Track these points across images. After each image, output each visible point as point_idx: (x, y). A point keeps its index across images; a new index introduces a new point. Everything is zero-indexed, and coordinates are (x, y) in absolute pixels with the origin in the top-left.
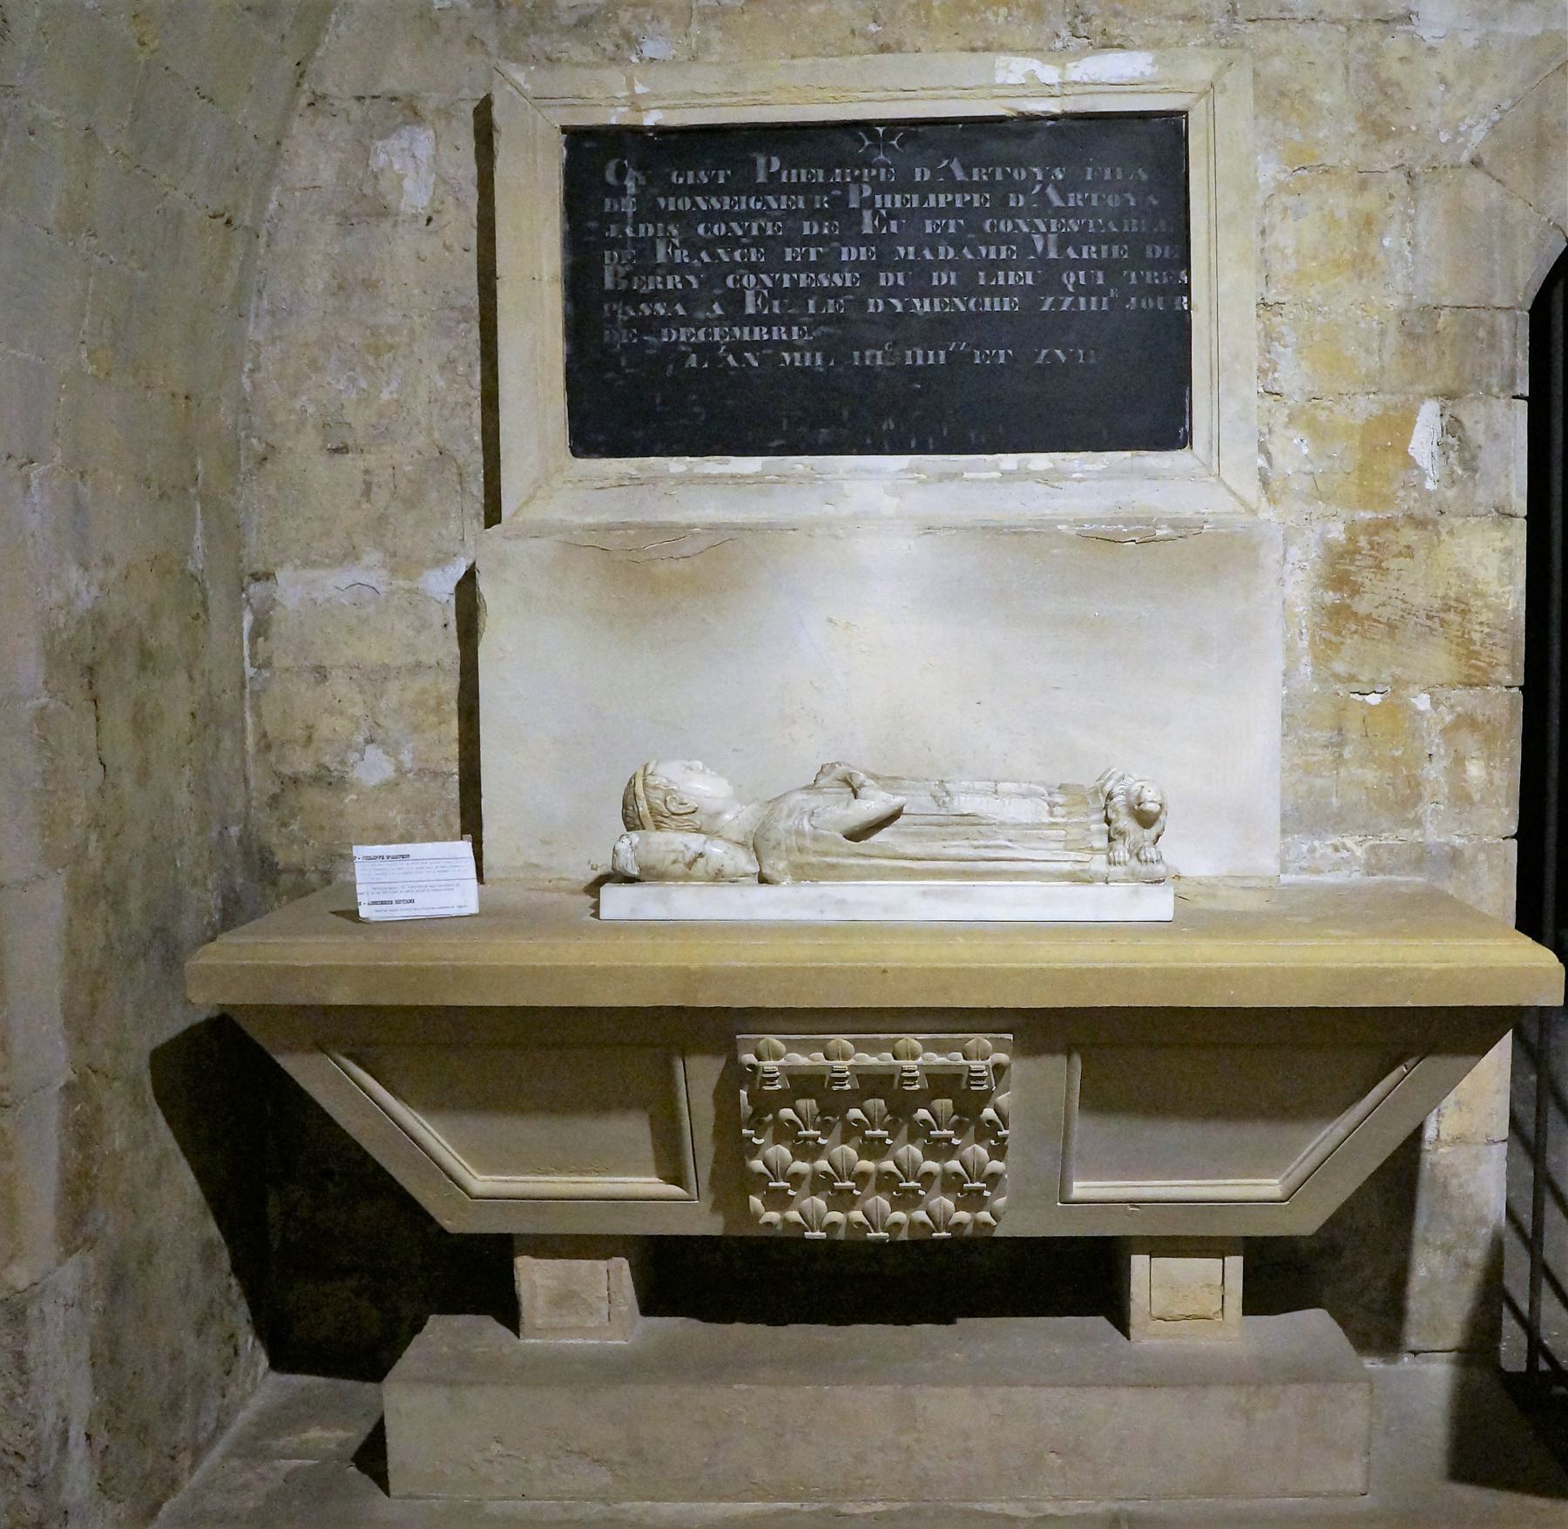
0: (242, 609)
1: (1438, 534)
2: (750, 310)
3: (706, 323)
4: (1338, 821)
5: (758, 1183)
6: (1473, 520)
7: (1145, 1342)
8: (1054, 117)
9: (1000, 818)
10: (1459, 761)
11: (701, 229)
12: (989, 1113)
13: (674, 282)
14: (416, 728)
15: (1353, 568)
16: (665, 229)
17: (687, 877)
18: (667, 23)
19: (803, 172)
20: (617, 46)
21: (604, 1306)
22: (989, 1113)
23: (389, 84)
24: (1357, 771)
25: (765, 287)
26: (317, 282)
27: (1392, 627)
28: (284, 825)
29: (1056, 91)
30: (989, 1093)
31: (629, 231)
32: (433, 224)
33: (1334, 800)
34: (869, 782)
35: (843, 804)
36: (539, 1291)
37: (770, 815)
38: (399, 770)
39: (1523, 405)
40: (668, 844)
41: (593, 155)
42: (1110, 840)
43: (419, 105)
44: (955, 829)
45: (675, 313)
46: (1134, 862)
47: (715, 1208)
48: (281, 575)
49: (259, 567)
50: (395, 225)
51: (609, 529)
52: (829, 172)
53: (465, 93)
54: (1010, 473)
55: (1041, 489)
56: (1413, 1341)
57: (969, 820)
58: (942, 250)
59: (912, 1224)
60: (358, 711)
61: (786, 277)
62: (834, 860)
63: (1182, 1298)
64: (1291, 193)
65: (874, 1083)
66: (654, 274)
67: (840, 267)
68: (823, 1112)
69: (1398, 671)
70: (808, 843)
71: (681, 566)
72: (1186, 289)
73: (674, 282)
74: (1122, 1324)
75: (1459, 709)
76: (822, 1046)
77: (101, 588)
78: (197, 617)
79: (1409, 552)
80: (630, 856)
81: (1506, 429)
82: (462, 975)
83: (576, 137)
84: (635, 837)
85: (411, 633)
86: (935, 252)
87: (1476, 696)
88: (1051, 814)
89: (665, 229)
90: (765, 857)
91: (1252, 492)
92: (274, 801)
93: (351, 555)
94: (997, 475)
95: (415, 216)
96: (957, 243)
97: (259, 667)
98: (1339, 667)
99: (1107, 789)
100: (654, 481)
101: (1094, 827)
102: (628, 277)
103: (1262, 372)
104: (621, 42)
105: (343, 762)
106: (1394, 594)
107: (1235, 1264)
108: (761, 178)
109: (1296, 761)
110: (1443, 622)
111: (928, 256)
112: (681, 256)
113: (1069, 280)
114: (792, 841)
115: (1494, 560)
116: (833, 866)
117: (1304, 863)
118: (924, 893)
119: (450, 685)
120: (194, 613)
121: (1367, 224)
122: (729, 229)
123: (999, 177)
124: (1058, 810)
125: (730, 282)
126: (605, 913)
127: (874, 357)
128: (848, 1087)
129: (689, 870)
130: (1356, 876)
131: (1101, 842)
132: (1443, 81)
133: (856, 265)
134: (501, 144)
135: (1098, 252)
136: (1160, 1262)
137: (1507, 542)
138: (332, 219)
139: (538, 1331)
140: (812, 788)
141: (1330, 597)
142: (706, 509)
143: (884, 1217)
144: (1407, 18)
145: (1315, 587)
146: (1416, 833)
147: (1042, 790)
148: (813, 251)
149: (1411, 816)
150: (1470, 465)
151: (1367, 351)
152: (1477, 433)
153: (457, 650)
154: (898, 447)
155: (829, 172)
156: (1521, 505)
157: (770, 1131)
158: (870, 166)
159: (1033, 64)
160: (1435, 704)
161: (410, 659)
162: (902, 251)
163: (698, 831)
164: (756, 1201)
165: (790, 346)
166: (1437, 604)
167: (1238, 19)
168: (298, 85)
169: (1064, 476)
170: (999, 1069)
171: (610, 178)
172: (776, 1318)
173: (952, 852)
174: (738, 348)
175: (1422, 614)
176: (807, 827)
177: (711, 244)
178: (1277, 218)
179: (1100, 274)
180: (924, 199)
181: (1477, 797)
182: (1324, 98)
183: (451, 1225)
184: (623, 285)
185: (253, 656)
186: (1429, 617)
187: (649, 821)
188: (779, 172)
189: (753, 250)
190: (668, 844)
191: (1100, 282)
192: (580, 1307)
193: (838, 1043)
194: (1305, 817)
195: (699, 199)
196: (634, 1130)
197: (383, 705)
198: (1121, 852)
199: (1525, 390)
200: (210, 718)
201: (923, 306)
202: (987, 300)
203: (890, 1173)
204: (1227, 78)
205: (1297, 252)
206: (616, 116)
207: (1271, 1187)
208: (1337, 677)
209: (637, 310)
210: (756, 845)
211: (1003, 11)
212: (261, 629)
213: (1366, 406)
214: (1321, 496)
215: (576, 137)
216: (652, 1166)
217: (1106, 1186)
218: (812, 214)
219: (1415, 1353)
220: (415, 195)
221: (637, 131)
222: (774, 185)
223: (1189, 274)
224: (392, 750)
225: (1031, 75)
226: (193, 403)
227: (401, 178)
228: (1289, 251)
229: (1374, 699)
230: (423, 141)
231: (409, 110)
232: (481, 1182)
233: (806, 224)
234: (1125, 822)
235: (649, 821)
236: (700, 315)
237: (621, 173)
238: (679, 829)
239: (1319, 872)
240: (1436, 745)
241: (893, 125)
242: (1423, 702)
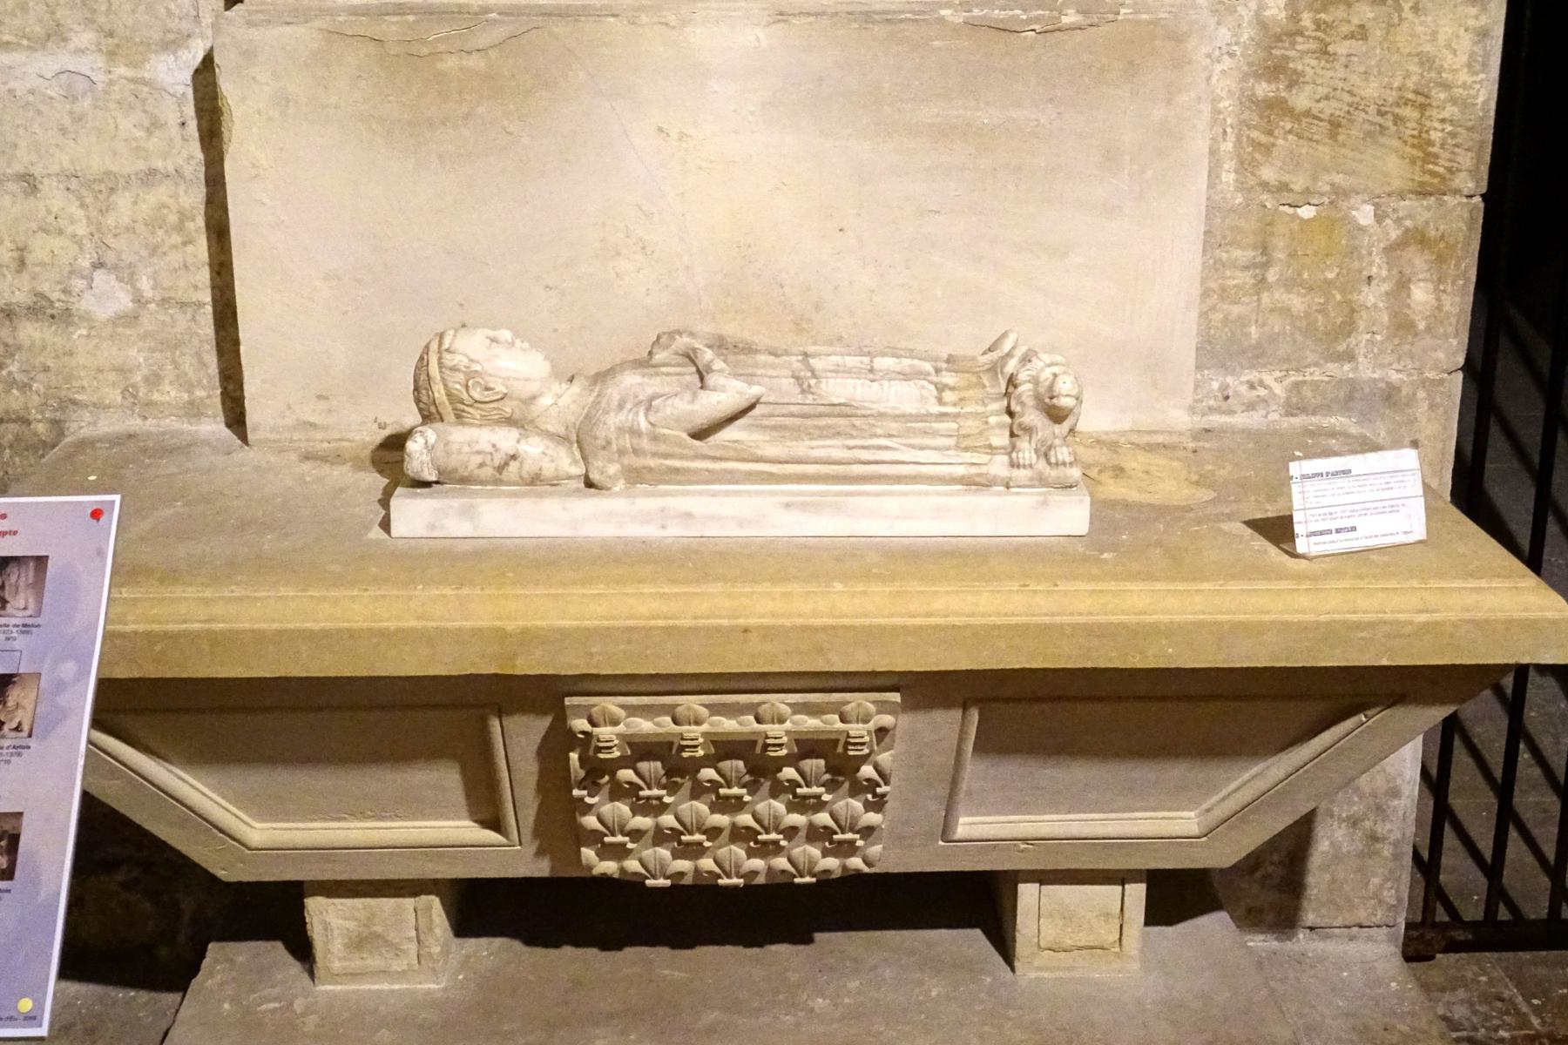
4: (1258, 355)
5: (594, 838)
9: (880, 407)
10: (1403, 284)
12: (867, 771)
14: (154, 250)
15: (1292, 53)
17: (497, 482)
21: (413, 947)
22: (867, 771)
24: (1280, 296)
27: (1335, 124)
33: (1253, 329)
34: (718, 365)
35: (688, 396)
36: (336, 933)
37: (596, 403)
38: (139, 300)
40: (472, 441)
42: (1012, 435)
46: (1041, 465)
47: (540, 853)
56: (1310, 918)
57: (845, 410)
59: (770, 871)
60: (81, 230)
62: (677, 463)
63: (1078, 937)
68: (669, 773)
69: (1338, 179)
70: (645, 444)
71: (475, 62)
74: (1003, 942)
75: (1408, 223)
76: (670, 710)
79: (1361, 33)
80: (426, 458)
82: (218, 642)
85: (140, 134)
87: (1428, 208)
88: (940, 401)
93: (55, 35)
98: (1269, 174)
99: (1011, 367)
101: (993, 420)
105: (65, 291)
106: (1341, 85)
107: (1137, 892)
109: (1213, 285)
110: (1398, 120)
114: (626, 441)
115: (1466, 42)
116: (677, 470)
118: (787, 505)
119: (195, 198)
124: (949, 396)
126: (398, 528)
128: (701, 753)
129: (500, 475)
130: (1274, 416)
136: (1047, 889)
137: (1483, 20)
139: (335, 977)
140: (644, 364)
141: (1263, 89)
143: (738, 866)
145: (1245, 77)
146: (1347, 367)
147: (928, 366)
149: (1341, 348)
153: (200, 156)
157: (606, 790)
160: (1379, 218)
161: (141, 165)
163: (510, 421)
164: (588, 854)
166: (1392, 97)
170: (882, 732)
172: (610, 943)
173: (821, 453)
175: (1372, 109)
176: (643, 424)
181: (1422, 326)
186: (1381, 114)
190: (472, 441)
193: (689, 709)
194: (1220, 349)
197: (110, 221)
198: (1026, 451)
203: (748, 828)
207: (1185, 821)
208: (1265, 185)
210: (581, 439)
216: (464, 811)
217: (994, 822)
219: (1311, 929)
224: (127, 275)
229: (1307, 212)
232: (259, 832)
234: (1032, 417)
235: (450, 416)
239: (1231, 412)
240: (1378, 266)
242: (1364, 215)
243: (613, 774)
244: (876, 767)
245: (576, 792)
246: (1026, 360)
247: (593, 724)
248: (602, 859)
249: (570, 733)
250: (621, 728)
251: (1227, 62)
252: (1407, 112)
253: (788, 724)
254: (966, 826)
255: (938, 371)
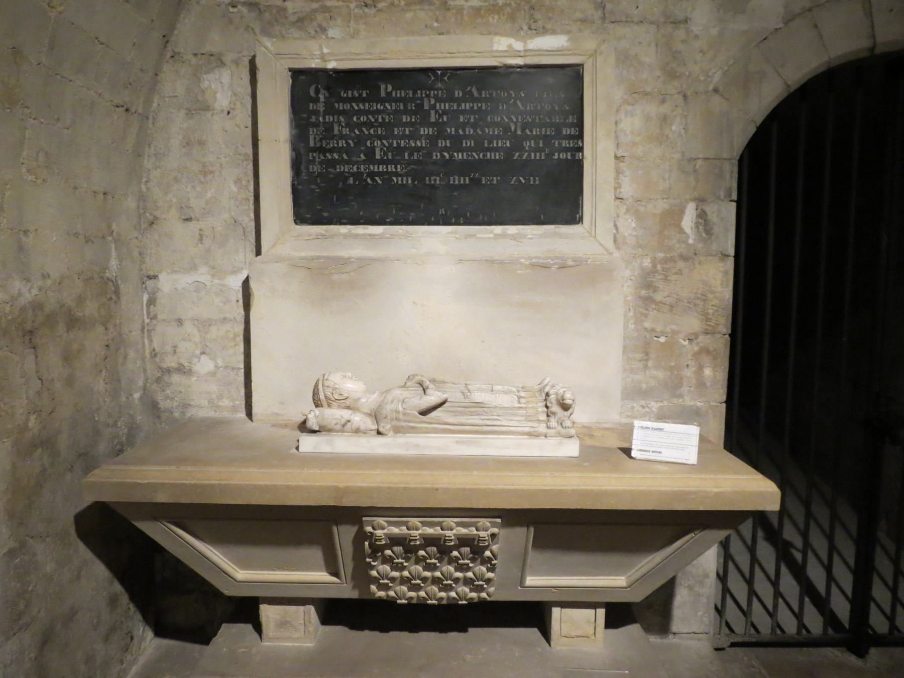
0: (143, 292)
1: (694, 264)
2: (378, 157)
3: (357, 163)
5: (375, 580)
6: (710, 258)
7: (558, 648)
8: (520, 67)
9: (494, 404)
10: (701, 368)
11: (355, 119)
13: (342, 143)
14: (224, 347)
16: (338, 119)
17: (343, 431)
18: (339, 21)
19: (403, 92)
20: (316, 31)
21: (302, 628)
22: (488, 553)
23: (208, 48)
24: (654, 372)
25: (385, 146)
26: (176, 141)
27: (672, 307)
28: (164, 391)
29: (522, 54)
30: (488, 546)
31: (321, 119)
32: (231, 115)
34: (431, 386)
37: (383, 401)
38: (217, 367)
39: (734, 205)
40: (334, 415)
41: (303, 79)
42: (548, 416)
43: (224, 59)
44: (472, 410)
45: (343, 158)
46: (560, 428)
47: (354, 587)
48: (162, 277)
49: (151, 273)
50: (212, 115)
51: (312, 259)
52: (415, 92)
53: (245, 53)
54: (498, 235)
55: (514, 242)
57: (479, 405)
58: (467, 130)
59: (448, 598)
60: (197, 339)
61: (395, 142)
62: (411, 424)
63: (578, 629)
64: (629, 104)
65: (429, 541)
66: (332, 139)
67: (420, 138)
68: (406, 552)
69: (674, 327)
70: (401, 416)
71: (344, 277)
72: (581, 149)
73: (342, 143)
74: (546, 634)
76: (405, 524)
77: (40, 290)
78: (111, 299)
79: (680, 272)
81: (726, 215)
82: (224, 489)
83: (296, 73)
84: (317, 411)
85: (221, 304)
86: (464, 131)
88: (519, 402)
89: (338, 119)
90: (380, 422)
91: (610, 244)
92: (158, 380)
93: (194, 267)
94: (492, 235)
95: (222, 111)
96: (474, 126)
97: (151, 319)
98: (647, 325)
99: (547, 389)
100: (333, 236)
102: (321, 140)
103: (615, 189)
104: (318, 29)
107: (601, 612)
108: (383, 94)
110: (695, 305)
111: (461, 132)
112: (346, 131)
113: (527, 144)
115: (719, 276)
116: (413, 427)
117: (629, 413)
118: (457, 442)
119: (240, 329)
120: (108, 296)
121: (664, 119)
122: (368, 118)
123: (494, 95)
124: (522, 400)
125: (368, 144)
126: (301, 449)
127: (435, 180)
128: (418, 543)
129: (344, 428)
131: (543, 417)
132: (701, 51)
133: (428, 136)
134: (260, 76)
135: (540, 132)
138: (183, 112)
140: (404, 386)
141: (644, 293)
142: (356, 251)
143: (435, 595)
144: (686, 21)
147: (514, 389)
148: (407, 130)
149: (678, 392)
150: (709, 232)
151: (664, 179)
152: (713, 217)
154: (445, 221)
155: (415, 92)
156: (731, 251)
157: (380, 559)
158: (434, 89)
159: (512, 41)
162: (449, 130)
163: (348, 408)
164: (373, 588)
165: (396, 174)
167: (607, 21)
168: (165, 47)
169: (525, 236)
170: (493, 536)
171: (312, 93)
172: (384, 629)
174: (372, 175)
176: (400, 409)
177: (359, 125)
178: (623, 117)
179: (541, 142)
180: (459, 105)
181: (708, 384)
182: (647, 60)
183: (227, 593)
184: (318, 145)
185: (148, 313)
186: (689, 303)
187: (324, 403)
188: (391, 92)
189: (379, 129)
190: (334, 415)
191: (541, 145)
192: (292, 631)
195: (354, 104)
196: (316, 554)
197: (209, 336)
198: (553, 422)
199: (735, 197)
200: (115, 347)
201: (459, 156)
202: (488, 154)
203: (438, 578)
204: (603, 47)
205: (632, 132)
206: (314, 64)
207: (620, 581)
208: (646, 329)
209: (325, 156)
210: (376, 416)
211: (496, 17)
212: (152, 302)
213: (662, 205)
214: (640, 246)
215: (296, 73)
216: (324, 568)
217: (540, 580)
218: (406, 112)
220: (222, 101)
221: (325, 71)
222: (389, 98)
223: (582, 142)
224: (213, 359)
225: (510, 46)
226: (109, 197)
227: (216, 93)
228: (628, 132)
230: (225, 75)
231: (216, 60)
232: (241, 575)
233: (404, 117)
234: (555, 408)
236: (354, 159)
237: (317, 92)
238: (339, 407)
241: (445, 70)
243: (383, 552)
244: (492, 552)
245: (368, 560)
246: (553, 386)
247: (374, 529)
248: (379, 590)
249: (365, 533)
250: (385, 531)
251: (630, 283)
252: (698, 302)
253: (454, 531)
254: (530, 581)
255: (518, 391)
